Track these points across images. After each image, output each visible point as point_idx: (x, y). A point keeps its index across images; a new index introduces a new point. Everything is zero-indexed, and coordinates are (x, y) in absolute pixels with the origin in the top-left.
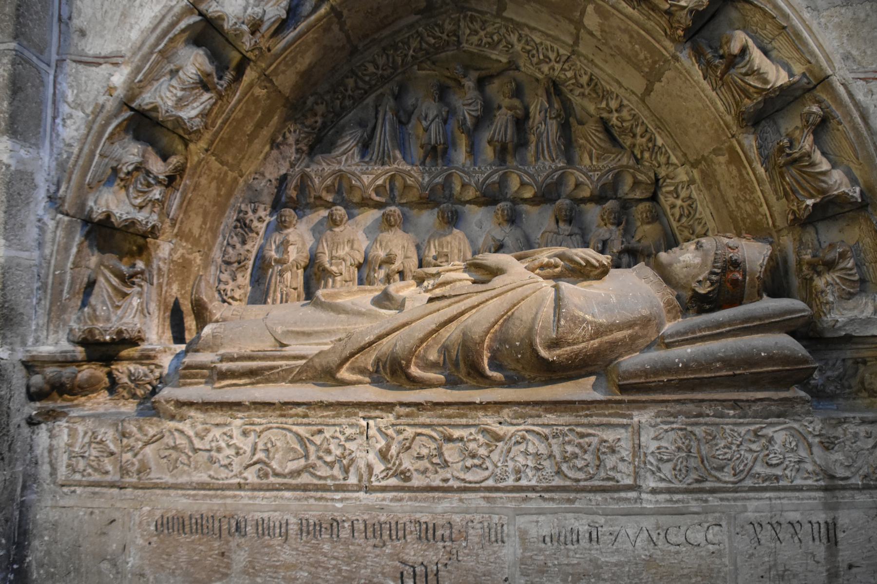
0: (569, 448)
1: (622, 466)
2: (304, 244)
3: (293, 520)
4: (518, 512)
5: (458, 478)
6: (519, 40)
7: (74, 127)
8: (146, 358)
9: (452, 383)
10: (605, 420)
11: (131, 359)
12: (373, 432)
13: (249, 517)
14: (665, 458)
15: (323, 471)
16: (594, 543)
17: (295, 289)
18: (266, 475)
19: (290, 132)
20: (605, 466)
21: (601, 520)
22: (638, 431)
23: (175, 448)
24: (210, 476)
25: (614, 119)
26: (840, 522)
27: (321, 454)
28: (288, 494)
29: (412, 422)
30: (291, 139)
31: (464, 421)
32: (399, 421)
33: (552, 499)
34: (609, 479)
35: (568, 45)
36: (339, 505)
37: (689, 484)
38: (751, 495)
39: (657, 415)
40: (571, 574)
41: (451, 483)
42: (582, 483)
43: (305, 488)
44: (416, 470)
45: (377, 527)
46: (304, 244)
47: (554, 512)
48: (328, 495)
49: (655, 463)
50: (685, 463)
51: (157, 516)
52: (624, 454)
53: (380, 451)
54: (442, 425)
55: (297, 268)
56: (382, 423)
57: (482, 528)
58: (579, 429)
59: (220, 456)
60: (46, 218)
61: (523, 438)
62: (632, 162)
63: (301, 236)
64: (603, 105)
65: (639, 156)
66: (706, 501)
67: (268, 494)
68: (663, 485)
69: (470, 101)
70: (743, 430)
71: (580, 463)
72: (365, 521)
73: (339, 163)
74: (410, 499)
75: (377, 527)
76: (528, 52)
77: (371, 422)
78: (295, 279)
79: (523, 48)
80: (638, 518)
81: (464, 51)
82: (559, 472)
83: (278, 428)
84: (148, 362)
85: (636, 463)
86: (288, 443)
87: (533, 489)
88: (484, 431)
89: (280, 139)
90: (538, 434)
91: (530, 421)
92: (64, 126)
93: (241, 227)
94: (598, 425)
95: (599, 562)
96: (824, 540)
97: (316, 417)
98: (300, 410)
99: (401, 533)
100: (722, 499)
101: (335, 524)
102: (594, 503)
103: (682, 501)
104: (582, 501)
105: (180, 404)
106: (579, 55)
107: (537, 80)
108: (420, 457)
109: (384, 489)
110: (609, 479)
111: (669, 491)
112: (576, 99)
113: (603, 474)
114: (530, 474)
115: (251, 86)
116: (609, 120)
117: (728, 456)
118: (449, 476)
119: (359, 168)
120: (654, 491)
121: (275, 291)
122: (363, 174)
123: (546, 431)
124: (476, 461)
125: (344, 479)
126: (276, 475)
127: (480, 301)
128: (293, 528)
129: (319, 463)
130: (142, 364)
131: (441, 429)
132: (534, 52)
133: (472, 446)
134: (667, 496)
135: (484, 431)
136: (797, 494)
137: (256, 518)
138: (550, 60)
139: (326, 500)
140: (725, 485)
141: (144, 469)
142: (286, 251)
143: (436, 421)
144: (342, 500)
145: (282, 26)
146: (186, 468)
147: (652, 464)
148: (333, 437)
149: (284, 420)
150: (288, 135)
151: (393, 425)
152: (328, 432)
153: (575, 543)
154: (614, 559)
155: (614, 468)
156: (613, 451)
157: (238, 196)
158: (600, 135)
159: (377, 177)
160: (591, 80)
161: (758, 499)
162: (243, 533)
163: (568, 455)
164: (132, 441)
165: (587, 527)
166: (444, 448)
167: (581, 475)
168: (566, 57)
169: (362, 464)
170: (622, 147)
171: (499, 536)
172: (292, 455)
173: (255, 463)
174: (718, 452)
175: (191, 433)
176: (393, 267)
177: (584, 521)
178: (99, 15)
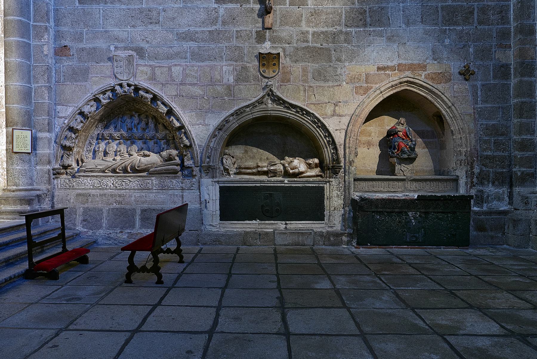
9: (124, 173)
15: (103, 186)
22: (152, 180)
51: (76, 193)
70: (169, 180)
71: (144, 185)
87: (136, 189)
97: (102, 178)
108: (119, 184)
109: (113, 189)
111: (157, 190)
120: (155, 190)
133: (127, 182)
178: (61, 109)
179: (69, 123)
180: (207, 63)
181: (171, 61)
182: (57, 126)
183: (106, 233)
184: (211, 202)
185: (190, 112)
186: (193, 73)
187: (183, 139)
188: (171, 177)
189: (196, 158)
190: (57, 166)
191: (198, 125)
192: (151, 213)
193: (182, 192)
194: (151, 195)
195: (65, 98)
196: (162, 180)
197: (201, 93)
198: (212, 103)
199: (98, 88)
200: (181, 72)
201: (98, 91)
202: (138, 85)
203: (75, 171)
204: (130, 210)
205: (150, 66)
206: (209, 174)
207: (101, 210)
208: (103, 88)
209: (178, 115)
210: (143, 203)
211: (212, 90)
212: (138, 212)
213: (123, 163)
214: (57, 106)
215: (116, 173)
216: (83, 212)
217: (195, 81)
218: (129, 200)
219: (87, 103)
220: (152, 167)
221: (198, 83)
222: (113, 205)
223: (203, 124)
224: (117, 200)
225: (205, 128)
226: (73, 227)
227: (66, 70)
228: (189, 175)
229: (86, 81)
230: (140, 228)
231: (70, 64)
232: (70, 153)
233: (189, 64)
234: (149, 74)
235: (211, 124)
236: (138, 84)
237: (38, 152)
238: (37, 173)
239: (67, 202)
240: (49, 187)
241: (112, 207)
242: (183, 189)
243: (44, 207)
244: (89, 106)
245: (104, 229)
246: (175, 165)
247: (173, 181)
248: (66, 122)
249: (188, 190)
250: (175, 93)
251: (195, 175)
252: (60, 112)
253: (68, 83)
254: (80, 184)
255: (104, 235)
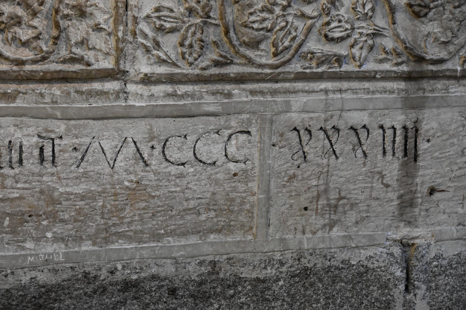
14: (168, 25)
16: (47, 165)
26: (424, 127)
34: (73, 60)
37: (203, 69)
38: (299, 85)
40: (8, 214)
42: (28, 67)
49: (150, 34)
50: (198, 35)
52: (101, 18)
66: (229, 95)
68: (162, 70)
80: (121, 123)
85: (120, 34)
95: (56, 194)
96: (399, 154)
100: (253, 93)
102: (47, 99)
103: (192, 96)
110: (73, 60)
113: (64, 53)
117: (268, 24)
134: (169, 88)
136: (367, 85)
140: (260, 71)
147: (145, 36)
153: (16, 165)
154: (80, 189)
155: (83, 43)
161: (309, 92)
165: (35, 139)
174: (253, 18)
177: (31, 130)
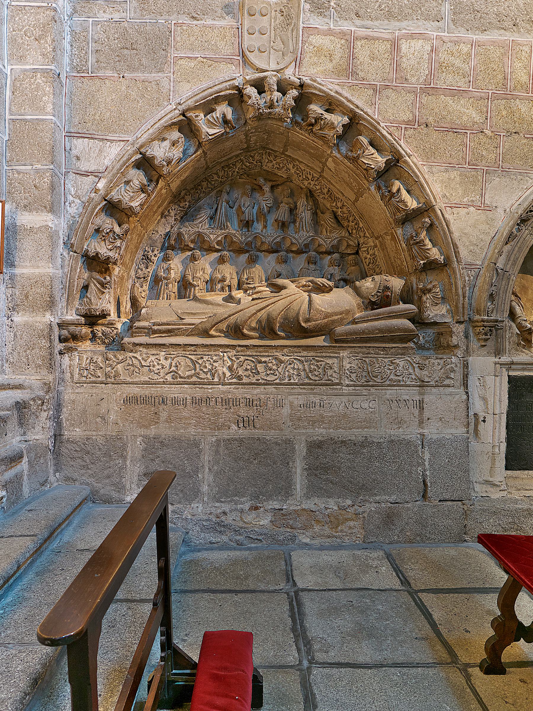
0: (312, 367)
1: (334, 375)
2: (178, 270)
3: (188, 397)
4: (290, 394)
5: (263, 379)
6: (293, 168)
7: (75, 208)
8: (111, 324)
9: (261, 338)
10: (328, 355)
11: (103, 325)
12: (226, 358)
13: (168, 396)
15: (203, 376)
17: (174, 293)
18: (176, 378)
19: (172, 210)
20: (328, 374)
21: (325, 397)
23: (133, 365)
24: (149, 378)
25: (339, 212)
27: (202, 368)
28: (186, 386)
29: (244, 354)
30: (173, 213)
31: (267, 354)
32: (238, 354)
33: (304, 388)
35: (318, 172)
36: (210, 391)
39: (351, 353)
41: (260, 381)
43: (194, 383)
44: (245, 376)
45: (227, 400)
46: (178, 270)
47: (305, 394)
48: (205, 386)
51: (125, 395)
52: (336, 369)
53: (229, 367)
54: (257, 356)
55: (175, 282)
56: (230, 354)
57: (274, 401)
58: (317, 359)
59: (154, 369)
60: (65, 254)
61: (293, 362)
62: (347, 234)
63: (176, 265)
64: (334, 204)
65: (350, 232)
67: (177, 386)
69: (267, 199)
71: (317, 373)
72: (222, 398)
73: (198, 228)
74: (242, 388)
75: (227, 400)
76: (298, 174)
77: (225, 354)
78: (174, 288)
79: (295, 172)
81: (264, 170)
82: (308, 377)
83: (182, 356)
84: (111, 326)
86: (186, 363)
87: (296, 384)
88: (276, 359)
89: (166, 213)
90: (299, 360)
91: (296, 354)
92: (70, 207)
93: (146, 259)
94: (325, 357)
98: (192, 348)
99: (238, 403)
101: (208, 399)
104: (317, 389)
105: (135, 345)
106: (324, 177)
107: (302, 188)
108: (247, 370)
109: (230, 384)
110: (329, 380)
112: (320, 199)
114: (295, 378)
115: (161, 189)
116: (337, 212)
118: (260, 378)
119: (208, 231)
120: (348, 386)
121: (163, 294)
122: (210, 234)
123: (303, 359)
124: (272, 372)
125: (213, 379)
126: (181, 377)
127: (276, 301)
128: (189, 401)
129: (201, 372)
130: (108, 327)
131: (256, 357)
132: (301, 174)
133: (270, 365)
135: (276, 359)
137: (171, 397)
138: (309, 179)
139: (205, 388)
141: (117, 375)
142: (169, 273)
143: (254, 354)
144: (211, 388)
145: (180, 160)
146: (138, 374)
148: (208, 361)
149: (185, 352)
150: (171, 211)
151: (235, 355)
152: (206, 358)
155: (331, 376)
156: (331, 368)
157: (144, 243)
158: (332, 220)
159: (218, 236)
160: (329, 191)
162: (165, 404)
163: (312, 369)
164: (111, 362)
166: (258, 366)
167: (317, 378)
168: (317, 178)
169: (221, 373)
170: (343, 227)
171: (281, 404)
172: (188, 369)
173: (171, 372)
175: (140, 358)
176: (225, 283)
178: (87, 149)
179: (109, 189)
180: (494, 35)
181: (397, 24)
182: (71, 198)
183: (211, 513)
184: (489, 419)
185: (447, 171)
186: (458, 62)
187: (425, 245)
188: (393, 350)
189: (461, 298)
190: (71, 316)
191: (466, 206)
192: (334, 451)
193: (421, 394)
194: (336, 401)
195: (97, 117)
196: (367, 360)
197: (477, 118)
198: (504, 147)
199: (196, 89)
200: (426, 56)
201: (198, 97)
202: (309, 86)
203: (115, 331)
204: (276, 444)
205: (343, 34)
206: (488, 343)
207: (196, 444)
208: (210, 90)
209: (417, 177)
210: (313, 422)
211: (504, 113)
212: (301, 449)
213: (262, 309)
214: (75, 141)
215: (238, 339)
216: (145, 450)
217: (462, 85)
218: (273, 414)
219: (160, 133)
220: (340, 322)
221: (471, 89)
222: (231, 431)
223: (479, 204)
224: (242, 414)
225: (483, 217)
226: (115, 495)
227: (103, 36)
228: (427, 345)
229: (161, 70)
230: (307, 496)
231: (116, 16)
232: (105, 278)
233: (446, 34)
234: (337, 57)
235: (498, 204)
236: (309, 82)
237: (17, 271)
238: (15, 335)
239: (99, 420)
240: (50, 378)
241: (225, 434)
242: (422, 384)
243: (37, 438)
244: (167, 143)
245: (205, 499)
246: (404, 318)
247: (397, 361)
248: (101, 185)
249: (437, 386)
250: (407, 116)
251: (456, 346)
252: (82, 159)
253: (109, 73)
254: (137, 370)
255: (205, 517)
